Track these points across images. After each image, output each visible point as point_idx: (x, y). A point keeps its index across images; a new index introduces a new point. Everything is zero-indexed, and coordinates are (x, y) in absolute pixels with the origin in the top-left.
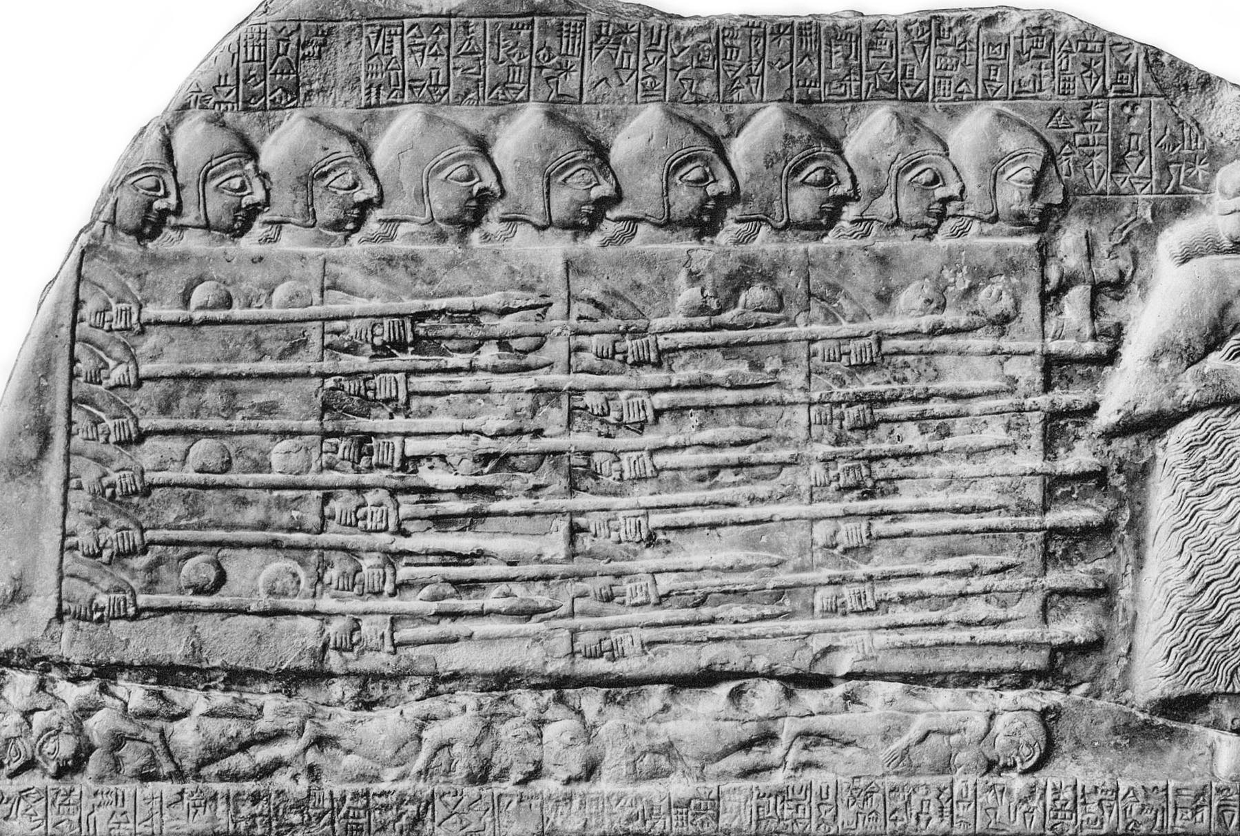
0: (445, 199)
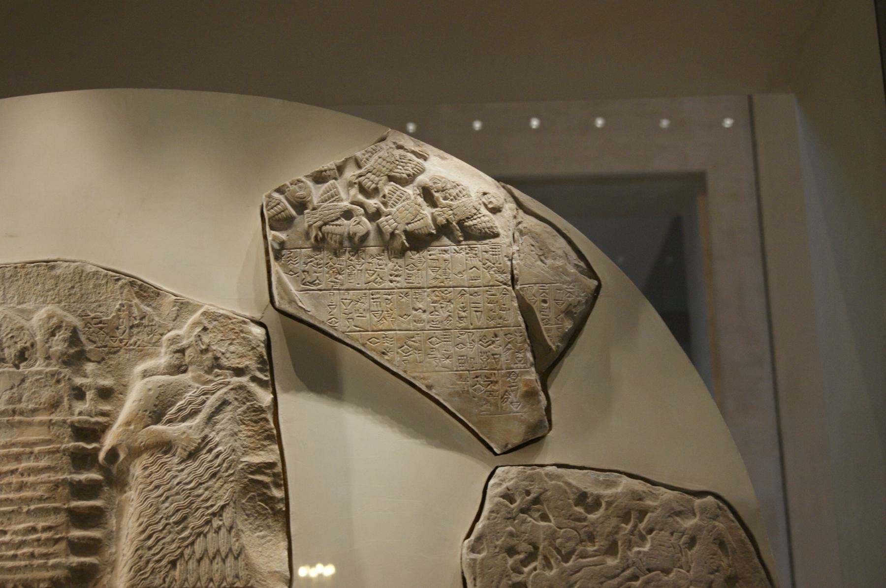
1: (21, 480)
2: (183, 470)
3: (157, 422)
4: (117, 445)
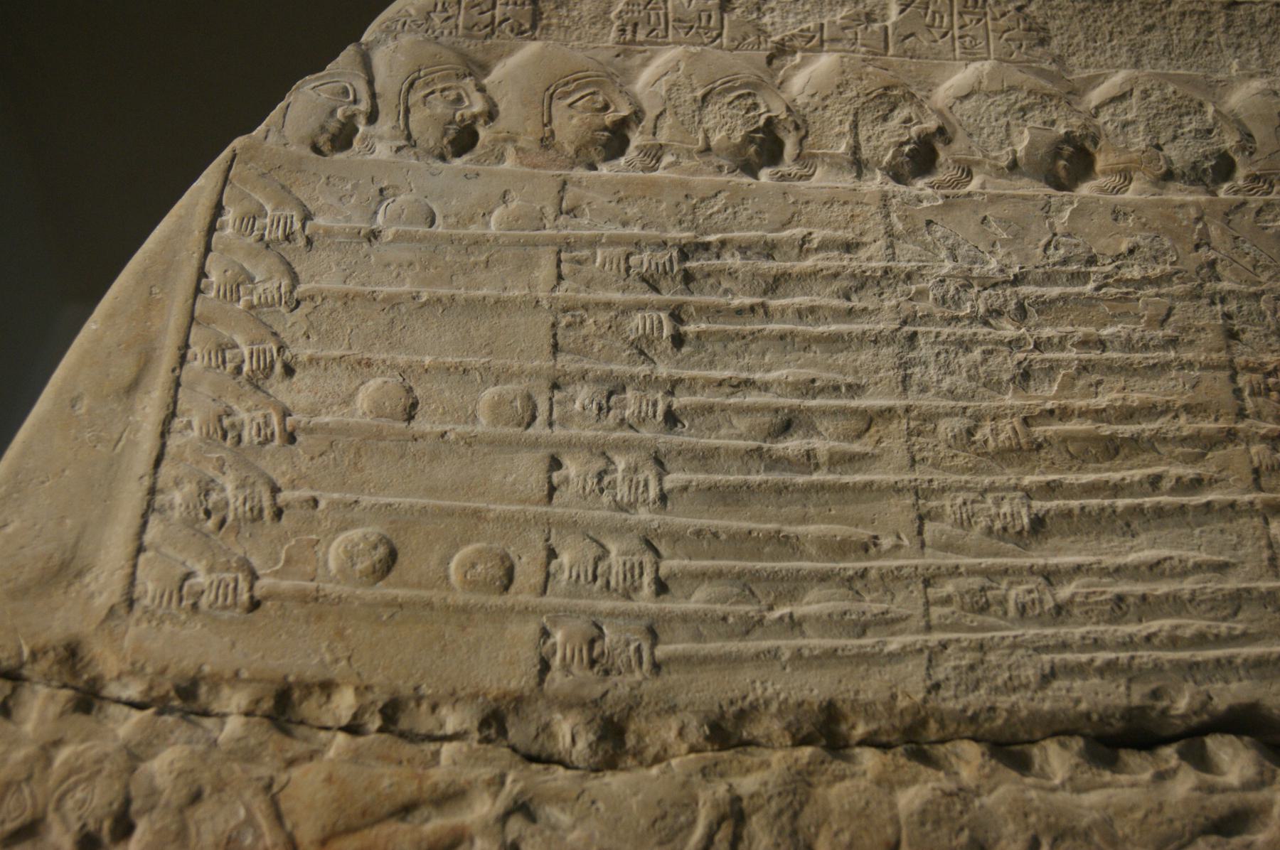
0: (726, 125)
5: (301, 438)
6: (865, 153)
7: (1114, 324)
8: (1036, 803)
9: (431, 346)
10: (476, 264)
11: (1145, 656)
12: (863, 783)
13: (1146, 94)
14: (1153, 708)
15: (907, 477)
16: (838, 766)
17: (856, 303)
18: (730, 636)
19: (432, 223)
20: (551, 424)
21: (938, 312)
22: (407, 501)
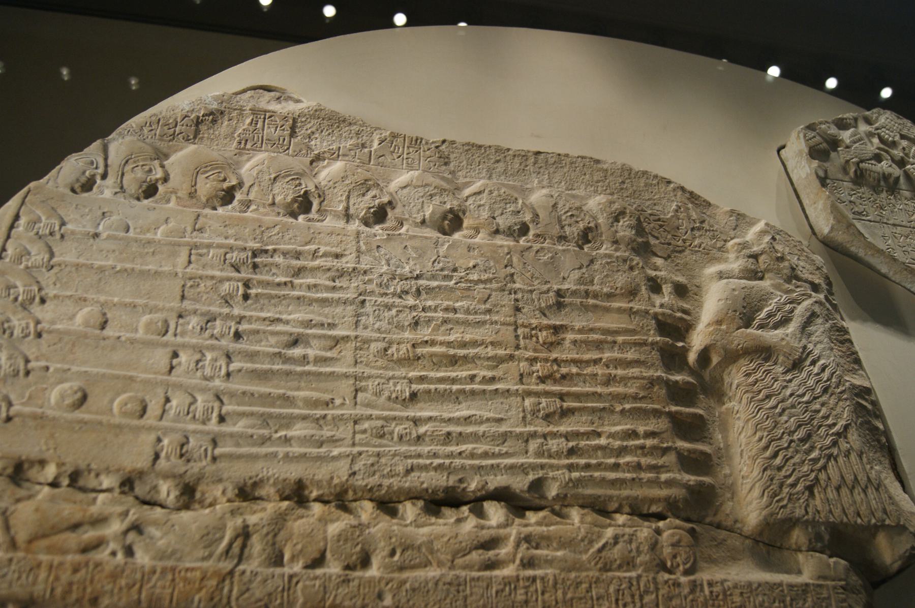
0: (284, 193)
1: (607, 371)
2: (790, 381)
3: (747, 325)
4: (710, 345)
5: (45, 335)
6: (352, 211)
7: (462, 301)
8: (396, 532)
9: (118, 293)
10: (147, 253)
11: (458, 462)
12: (312, 520)
13: (491, 192)
14: (459, 487)
15: (352, 370)
16: (301, 511)
17: (338, 284)
18: (254, 445)
19: (128, 231)
20: (175, 335)
21: (377, 290)
22: (95, 370)
